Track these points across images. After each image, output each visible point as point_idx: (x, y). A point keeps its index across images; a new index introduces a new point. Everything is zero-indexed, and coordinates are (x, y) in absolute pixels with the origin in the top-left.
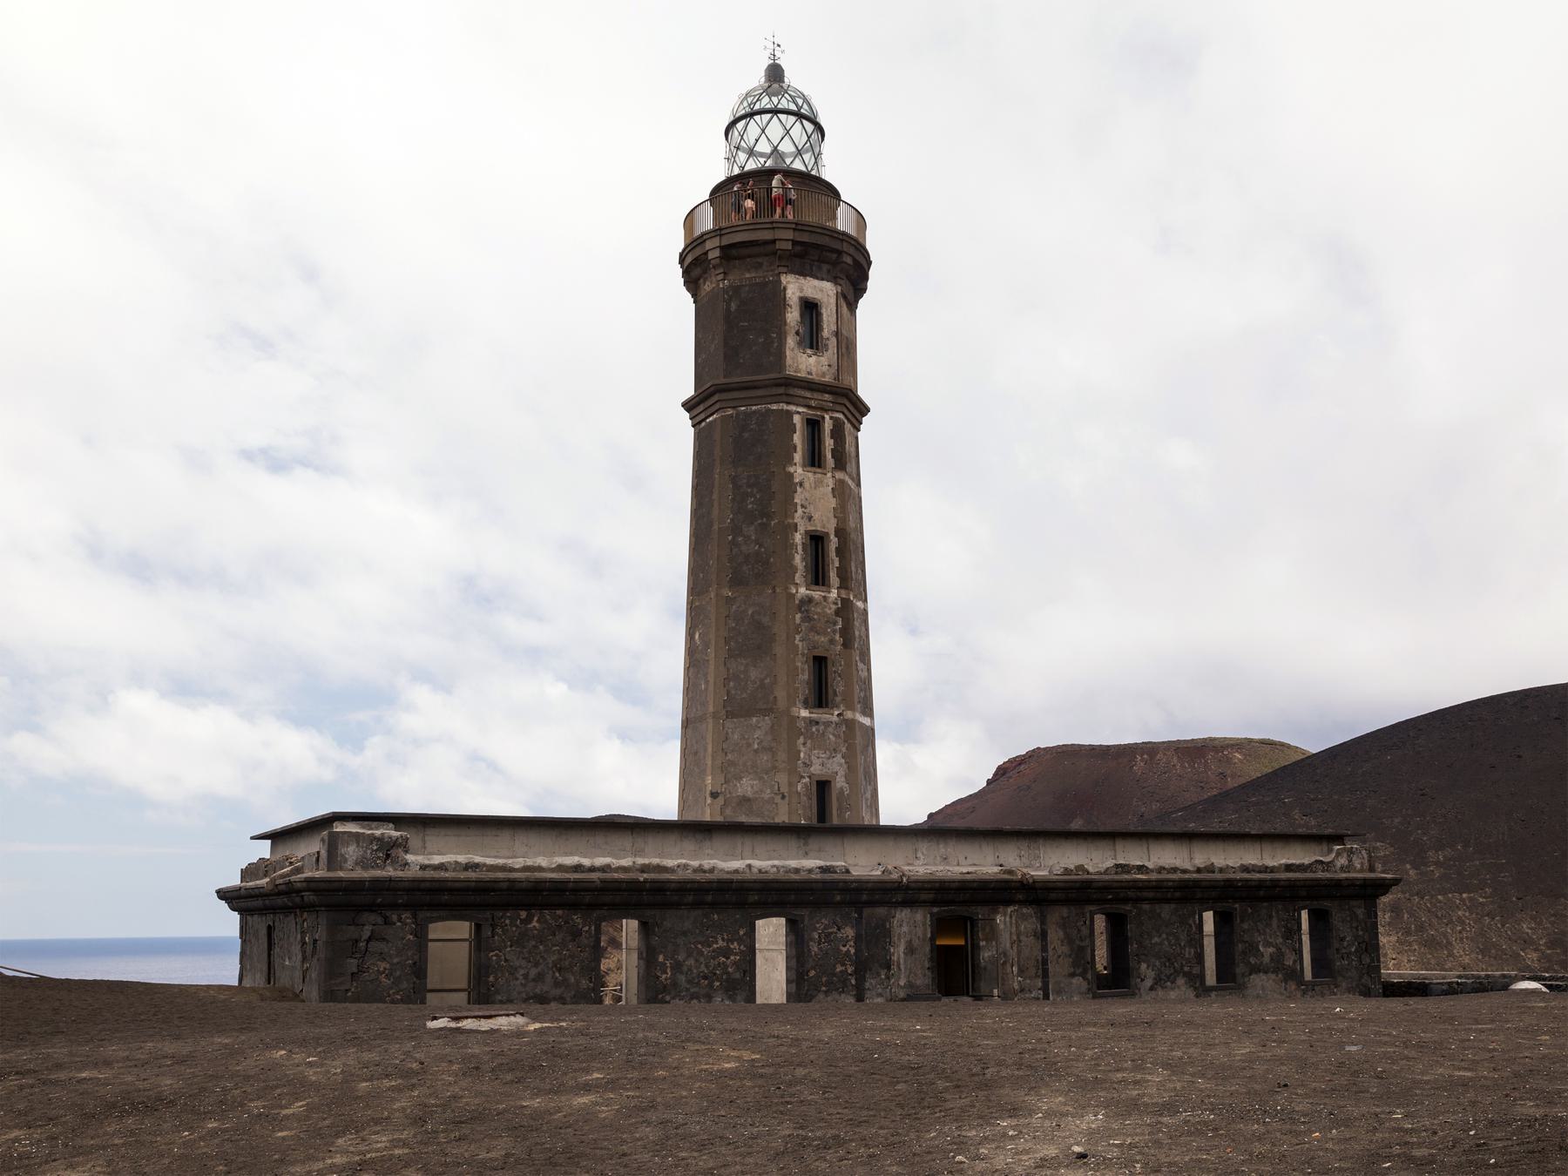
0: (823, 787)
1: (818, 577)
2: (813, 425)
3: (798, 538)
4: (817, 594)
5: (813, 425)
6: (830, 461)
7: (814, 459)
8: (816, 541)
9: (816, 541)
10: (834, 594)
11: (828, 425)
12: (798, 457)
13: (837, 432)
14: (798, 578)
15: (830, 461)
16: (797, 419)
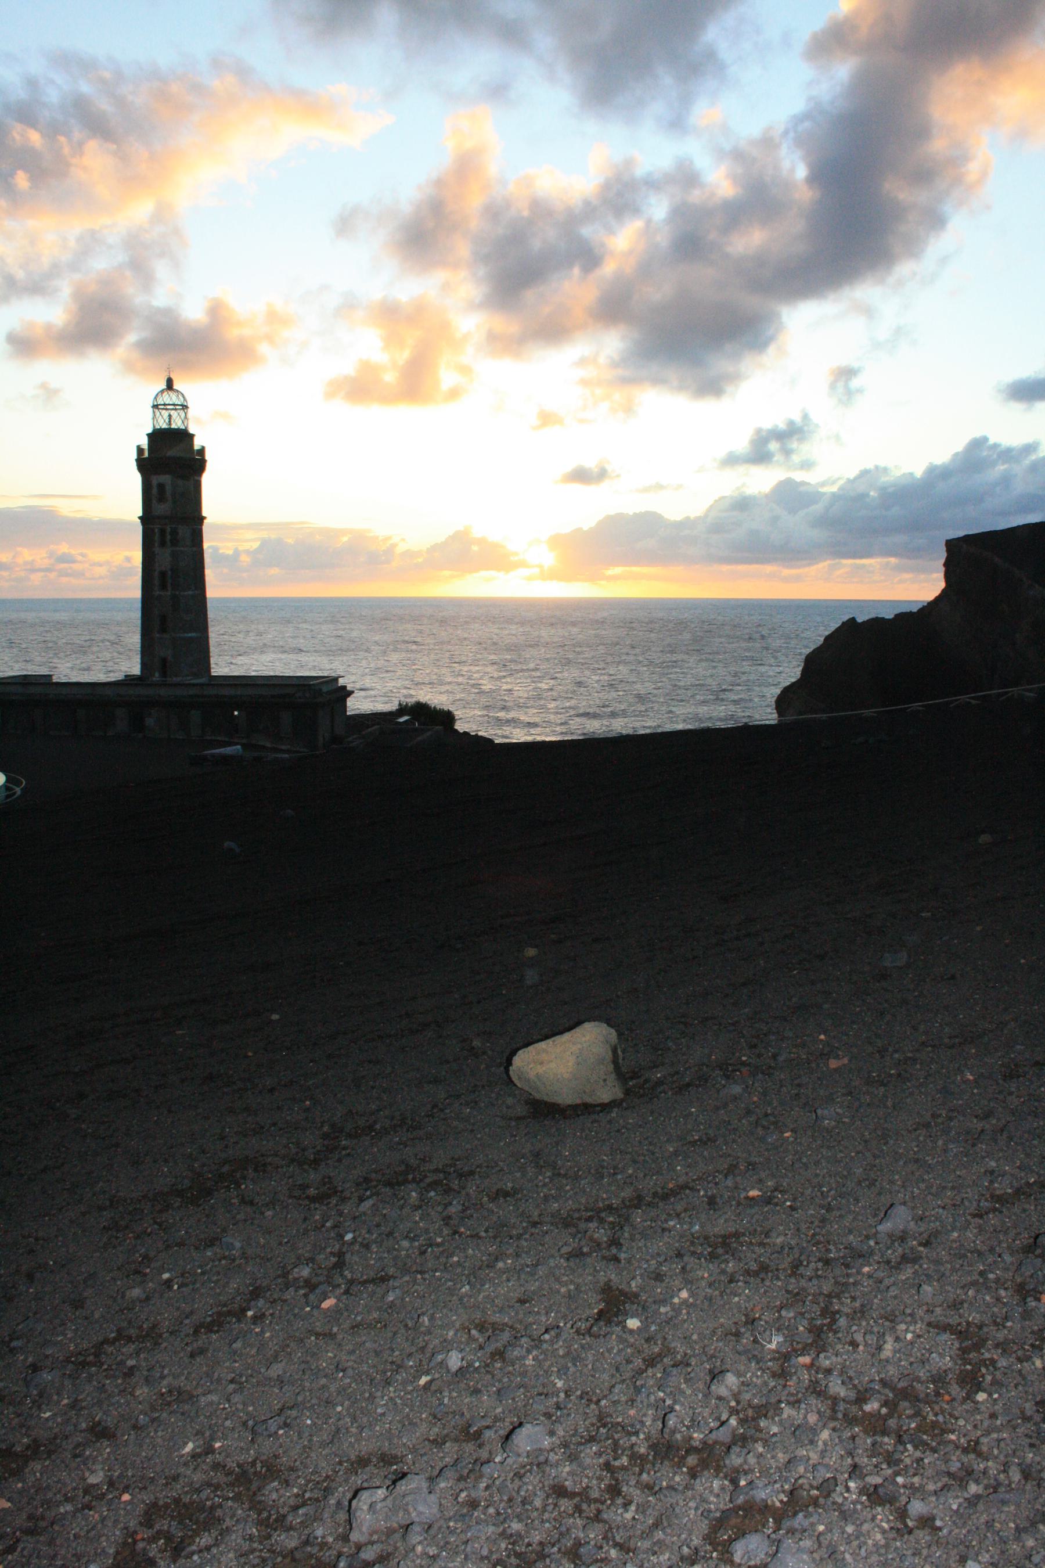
0: (164, 661)
1: (163, 586)
2: (163, 532)
3: (156, 573)
4: (162, 593)
5: (163, 532)
6: (169, 543)
7: (163, 544)
8: (163, 575)
9: (163, 575)
10: (169, 593)
11: (169, 530)
12: (156, 545)
13: (174, 532)
14: (156, 588)
15: (169, 543)
16: (156, 530)
